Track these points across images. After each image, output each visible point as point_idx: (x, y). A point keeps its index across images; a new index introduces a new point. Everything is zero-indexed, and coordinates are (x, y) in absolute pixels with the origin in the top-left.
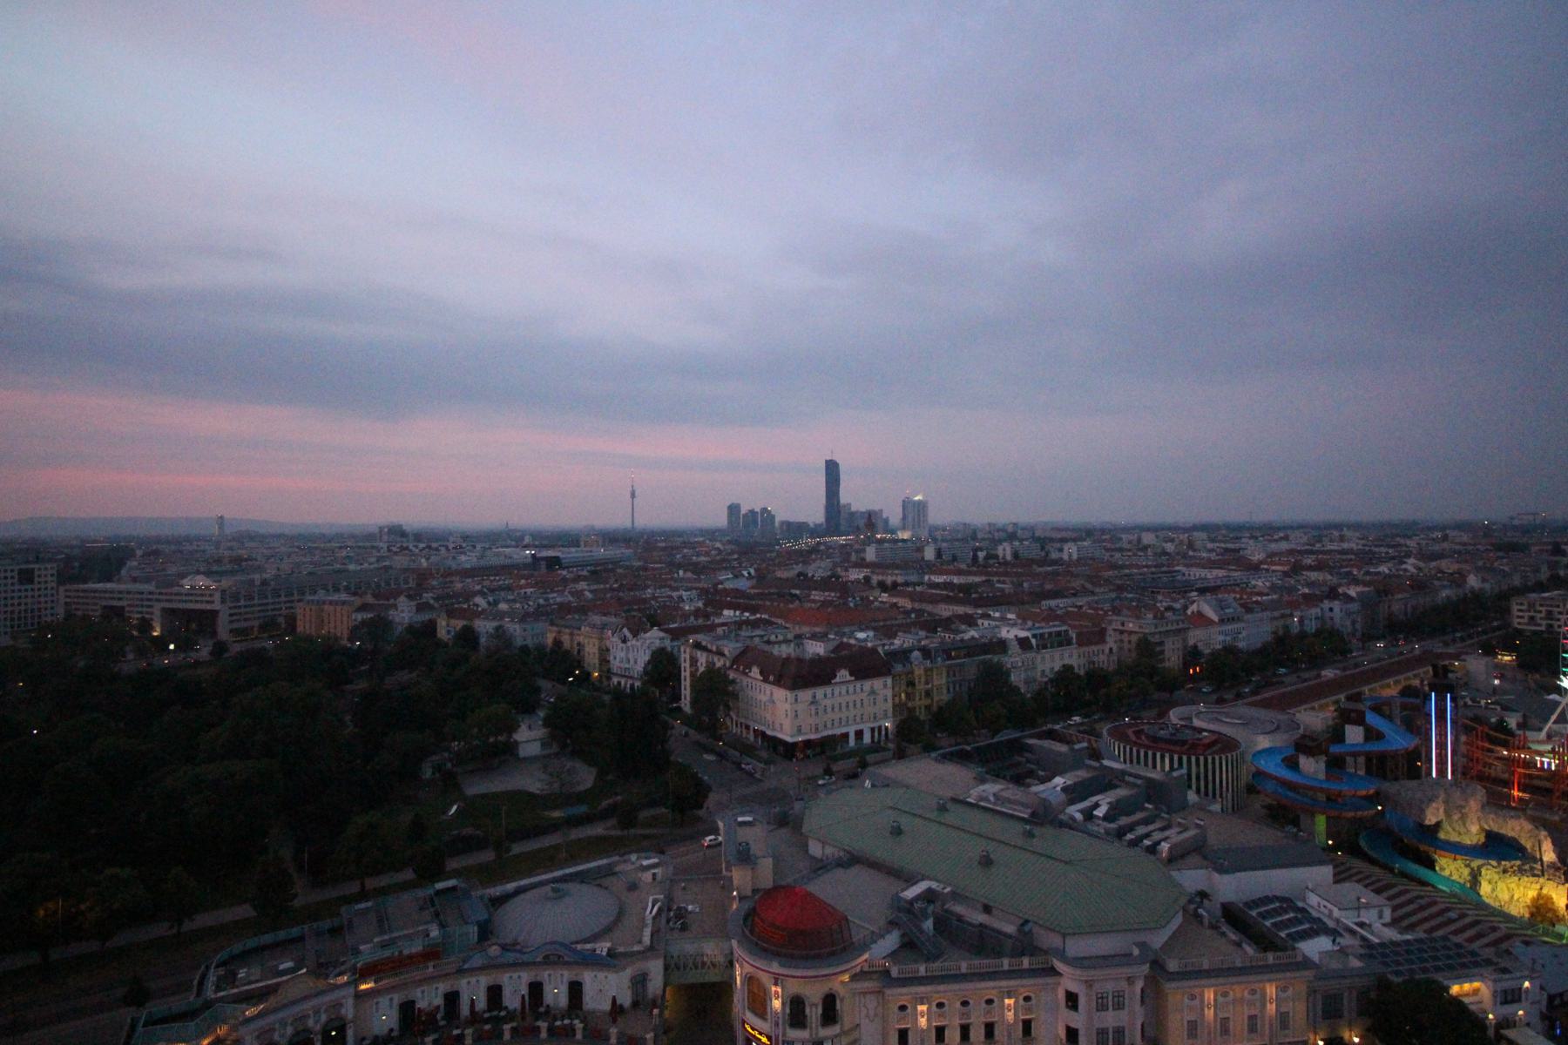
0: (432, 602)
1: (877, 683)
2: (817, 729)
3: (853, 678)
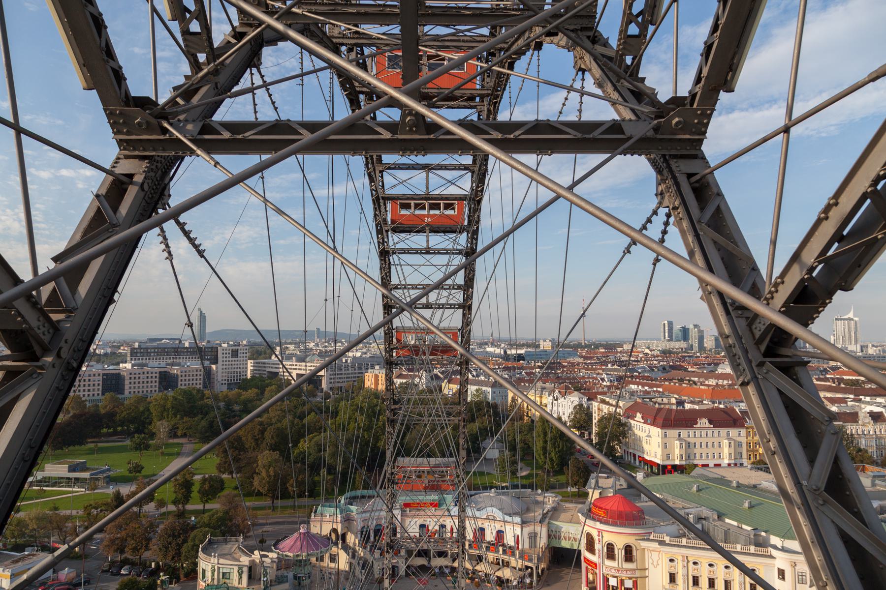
0: (439, 374)
1: (733, 432)
2: (681, 458)
3: (712, 426)
